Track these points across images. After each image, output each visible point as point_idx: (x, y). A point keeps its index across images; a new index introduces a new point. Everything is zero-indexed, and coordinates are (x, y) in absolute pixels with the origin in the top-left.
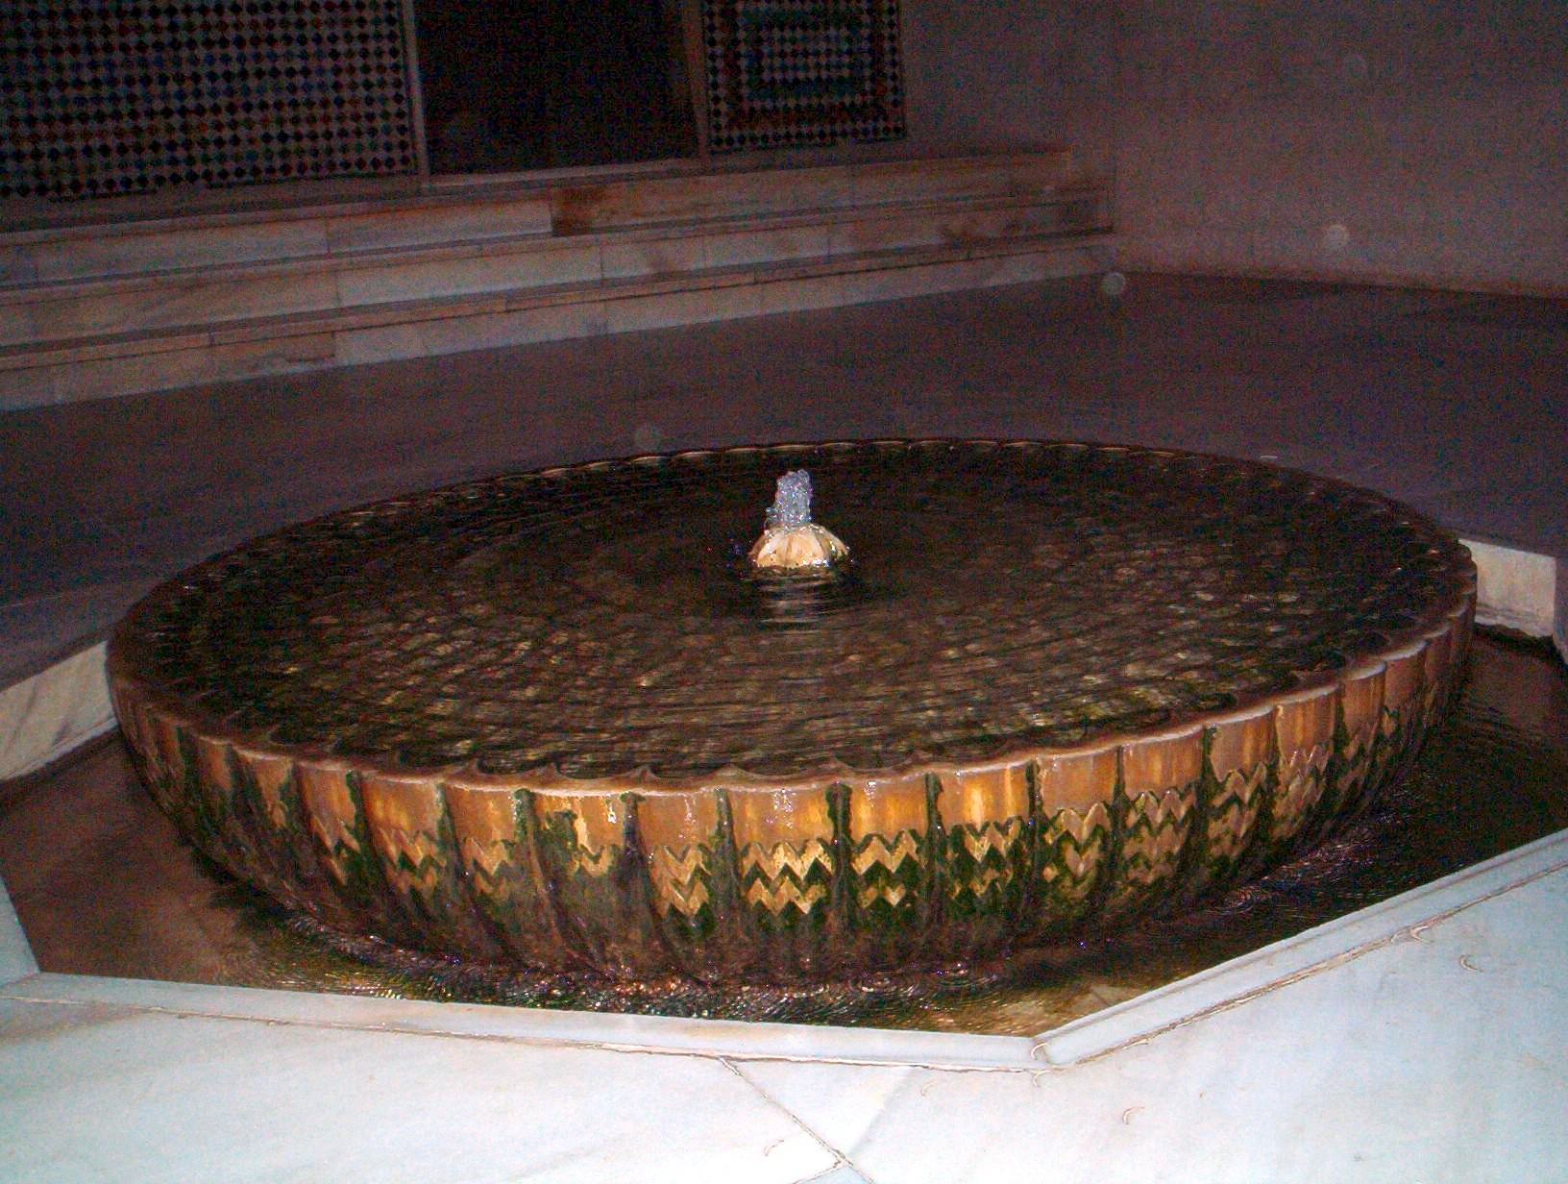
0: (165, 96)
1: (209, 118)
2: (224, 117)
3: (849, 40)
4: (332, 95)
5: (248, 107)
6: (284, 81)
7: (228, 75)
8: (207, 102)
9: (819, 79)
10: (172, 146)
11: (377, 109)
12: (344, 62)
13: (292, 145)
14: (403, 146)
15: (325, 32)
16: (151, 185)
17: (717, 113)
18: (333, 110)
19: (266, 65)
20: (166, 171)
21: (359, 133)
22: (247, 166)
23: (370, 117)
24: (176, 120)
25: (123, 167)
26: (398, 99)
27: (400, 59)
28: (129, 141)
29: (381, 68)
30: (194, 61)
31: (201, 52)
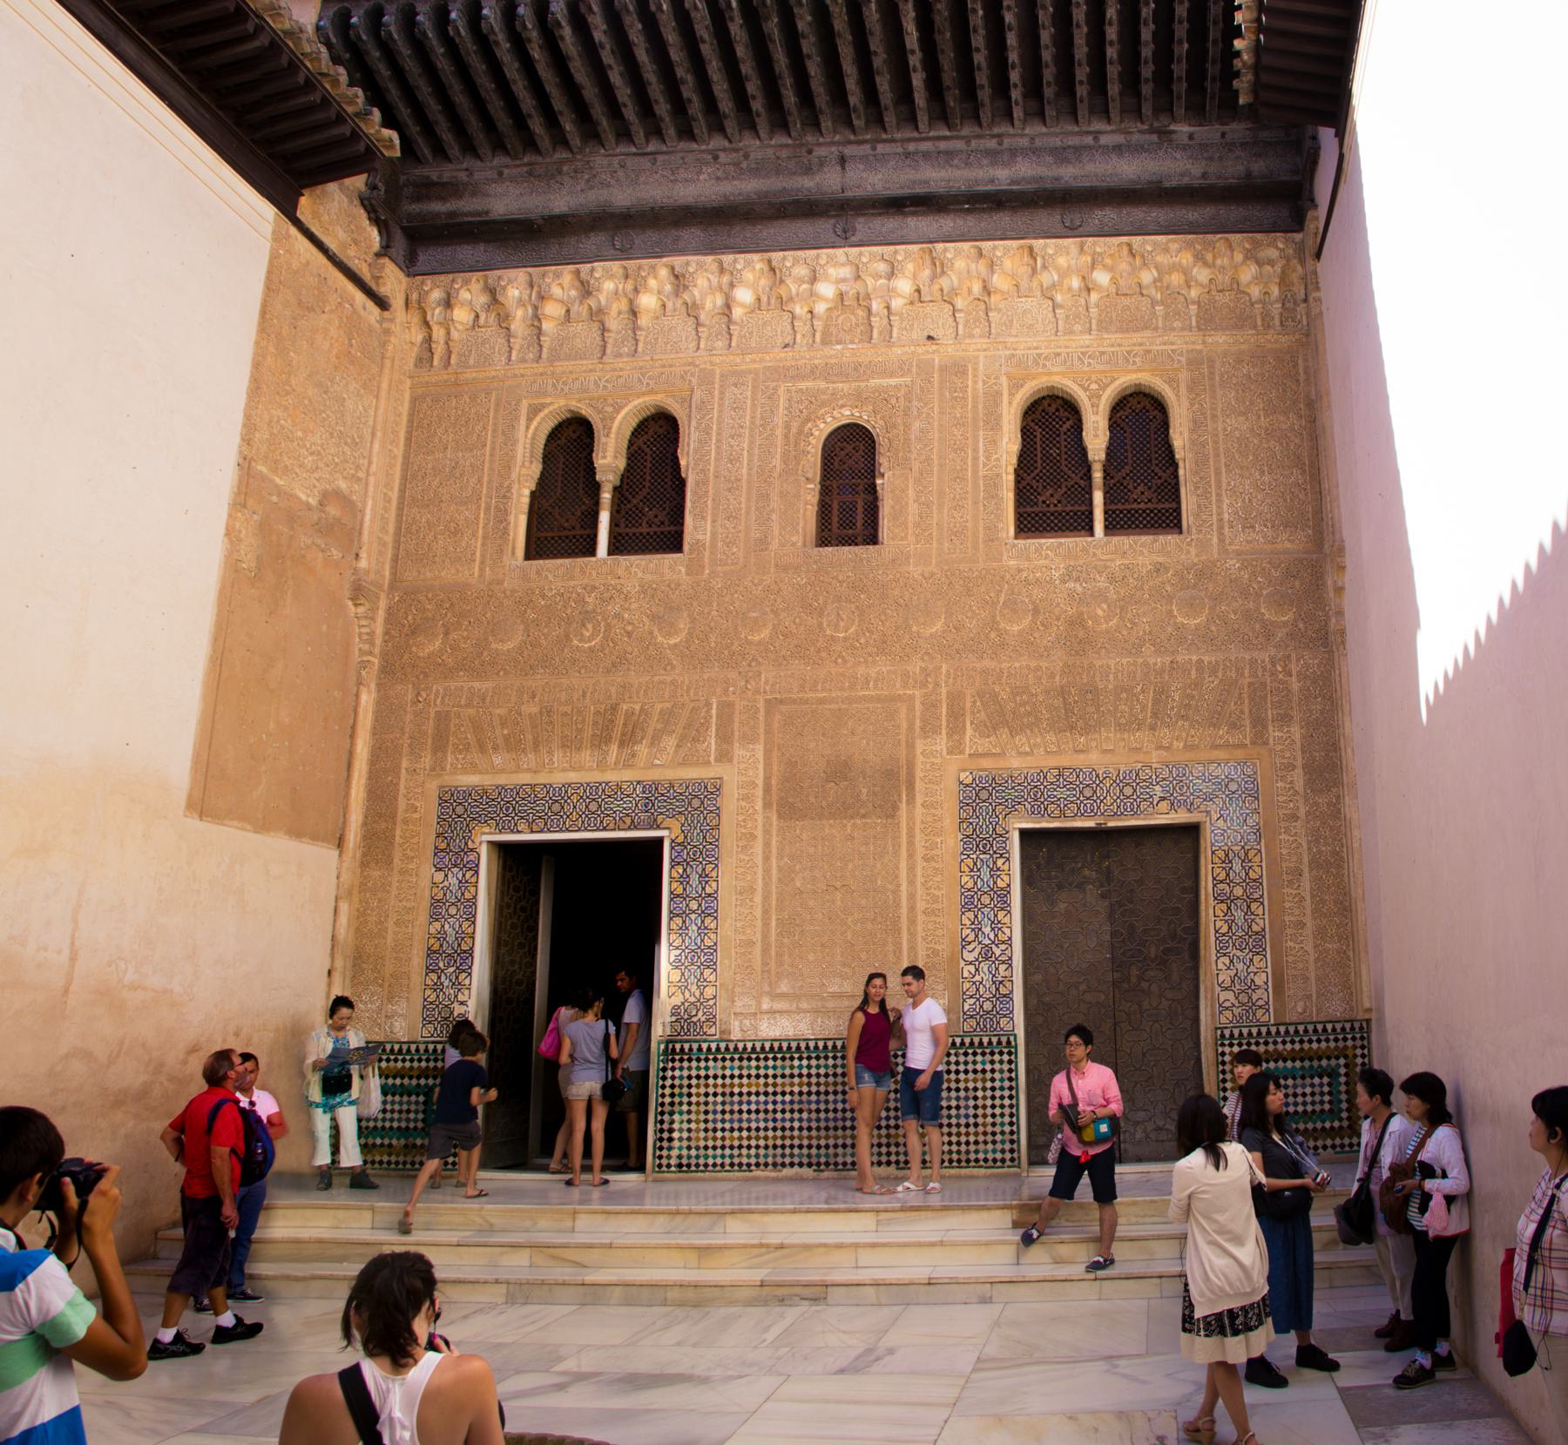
4: (972, 1121)
11: (998, 1129)
14: (1012, 1151)
15: (971, 1085)
18: (972, 1129)
21: (985, 1143)
23: (994, 1134)
26: (1011, 1124)
27: (1014, 1101)
29: (1002, 1106)
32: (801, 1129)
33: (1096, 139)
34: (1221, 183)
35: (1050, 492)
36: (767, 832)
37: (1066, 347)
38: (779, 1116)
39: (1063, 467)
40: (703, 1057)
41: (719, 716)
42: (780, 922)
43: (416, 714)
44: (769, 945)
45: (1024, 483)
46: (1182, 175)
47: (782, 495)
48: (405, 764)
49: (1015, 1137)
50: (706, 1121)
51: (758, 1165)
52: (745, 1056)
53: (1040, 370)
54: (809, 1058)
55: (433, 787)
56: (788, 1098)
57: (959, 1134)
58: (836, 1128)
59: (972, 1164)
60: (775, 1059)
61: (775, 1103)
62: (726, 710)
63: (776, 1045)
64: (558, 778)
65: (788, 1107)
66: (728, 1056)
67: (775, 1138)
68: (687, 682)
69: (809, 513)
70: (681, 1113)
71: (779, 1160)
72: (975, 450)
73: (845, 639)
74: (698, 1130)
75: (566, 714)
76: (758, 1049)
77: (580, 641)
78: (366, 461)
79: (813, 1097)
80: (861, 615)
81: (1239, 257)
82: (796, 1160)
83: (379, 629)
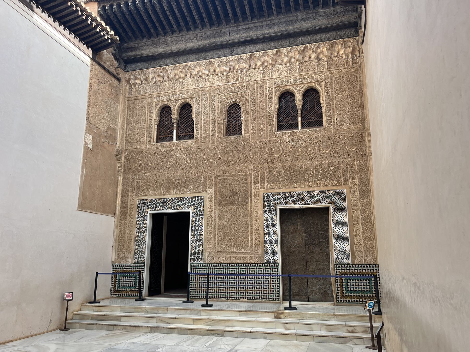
0: (243, 286)
1: (249, 289)
2: (251, 289)
3: (369, 283)
4: (267, 287)
5: (255, 288)
6: (260, 284)
7: (252, 283)
8: (249, 287)
9: (362, 290)
10: (243, 293)
11: (274, 290)
12: (269, 282)
13: (260, 294)
14: (278, 296)
16: (240, 299)
17: (338, 295)
18: (267, 290)
19: (258, 282)
20: (242, 297)
21: (271, 293)
22: (254, 297)
23: (273, 291)
24: (244, 289)
25: (236, 295)
26: (278, 289)
27: (279, 282)
28: (238, 292)
29: (275, 284)
30: (248, 281)
31: (249, 279)
32: (223, 288)
33: (297, 17)
34: (333, 25)
36: (215, 209)
38: (218, 284)
40: (199, 268)
41: (203, 181)
42: (219, 233)
43: (132, 182)
44: (216, 239)
46: (322, 24)
47: (218, 124)
48: (130, 194)
49: (279, 292)
50: (199, 285)
51: (212, 297)
52: (209, 268)
53: (283, 85)
54: (225, 269)
55: (136, 199)
56: (220, 279)
57: (264, 291)
58: (232, 288)
59: (267, 299)
60: (217, 269)
61: (217, 280)
62: (205, 178)
63: (217, 265)
64: (166, 197)
65: (220, 282)
66: (205, 268)
67: (217, 290)
68: (195, 172)
69: (224, 128)
70: (193, 283)
71: (218, 296)
72: (267, 109)
74: (197, 287)
75: (167, 181)
76: (213, 266)
77: (170, 163)
78: (117, 120)
79: (226, 279)
80: (238, 153)
81: (340, 46)
82: (222, 296)
83: (123, 162)
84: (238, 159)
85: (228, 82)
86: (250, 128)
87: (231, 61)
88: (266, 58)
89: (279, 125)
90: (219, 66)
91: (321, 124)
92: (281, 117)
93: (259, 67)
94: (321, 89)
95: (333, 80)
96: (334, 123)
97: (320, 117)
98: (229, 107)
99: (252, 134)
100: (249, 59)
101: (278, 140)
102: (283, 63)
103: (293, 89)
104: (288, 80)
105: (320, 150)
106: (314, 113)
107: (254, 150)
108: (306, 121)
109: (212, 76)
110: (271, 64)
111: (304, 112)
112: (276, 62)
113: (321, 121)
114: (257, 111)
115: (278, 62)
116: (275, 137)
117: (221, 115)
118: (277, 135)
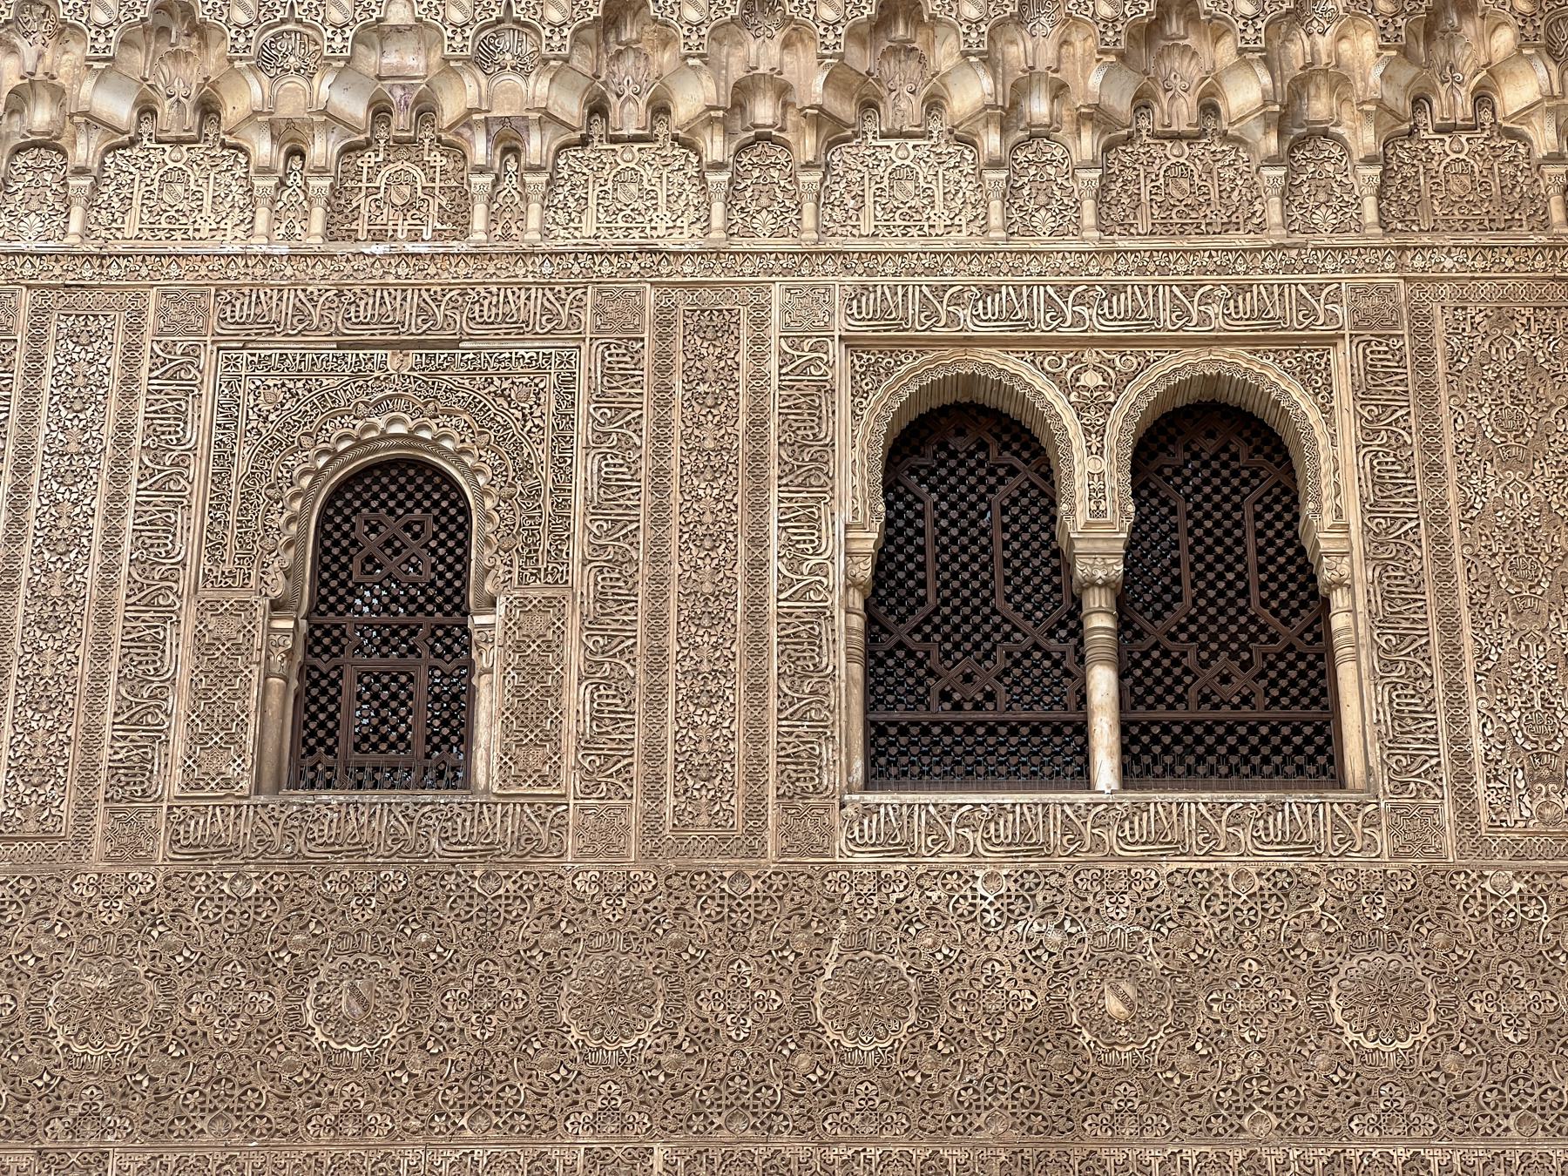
35: (966, 665)
37: (1013, 269)
39: (998, 602)
45: (888, 642)
47: (203, 647)
53: (940, 332)
69: (274, 700)
72: (758, 542)
73: (368, 1064)
80: (420, 992)
81: (1504, 39)
84: (416, 1057)
85: (351, 236)
86: (569, 724)
87: (397, 29)
88: (774, 49)
89: (882, 731)
90: (266, 61)
91: (1311, 760)
92: (900, 645)
93: (691, 127)
94: (1314, 416)
95: (1439, 345)
96: (1462, 757)
97: (1304, 692)
98: (337, 492)
99: (590, 787)
100: (590, 34)
101: (882, 881)
102: (934, 126)
103: (1040, 382)
104: (991, 290)
105: (1321, 1016)
106: (1244, 647)
107: (611, 969)
108: (1161, 713)
109: (174, 157)
110: (821, 118)
111: (1142, 621)
112: (869, 105)
113: (1319, 731)
114: (658, 558)
115: (887, 110)
116: (841, 842)
117: (247, 557)
118: (871, 826)
